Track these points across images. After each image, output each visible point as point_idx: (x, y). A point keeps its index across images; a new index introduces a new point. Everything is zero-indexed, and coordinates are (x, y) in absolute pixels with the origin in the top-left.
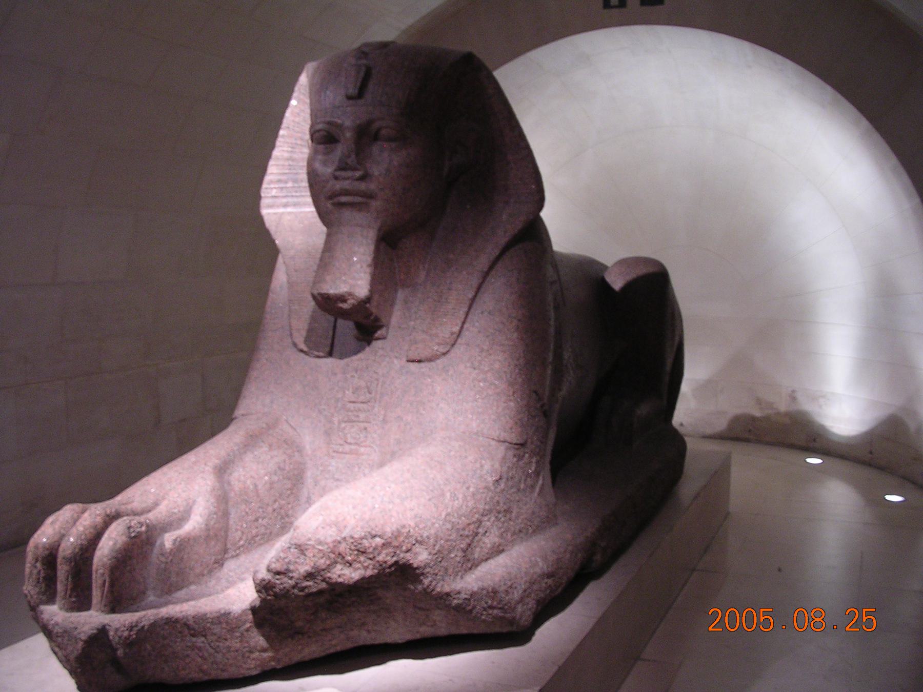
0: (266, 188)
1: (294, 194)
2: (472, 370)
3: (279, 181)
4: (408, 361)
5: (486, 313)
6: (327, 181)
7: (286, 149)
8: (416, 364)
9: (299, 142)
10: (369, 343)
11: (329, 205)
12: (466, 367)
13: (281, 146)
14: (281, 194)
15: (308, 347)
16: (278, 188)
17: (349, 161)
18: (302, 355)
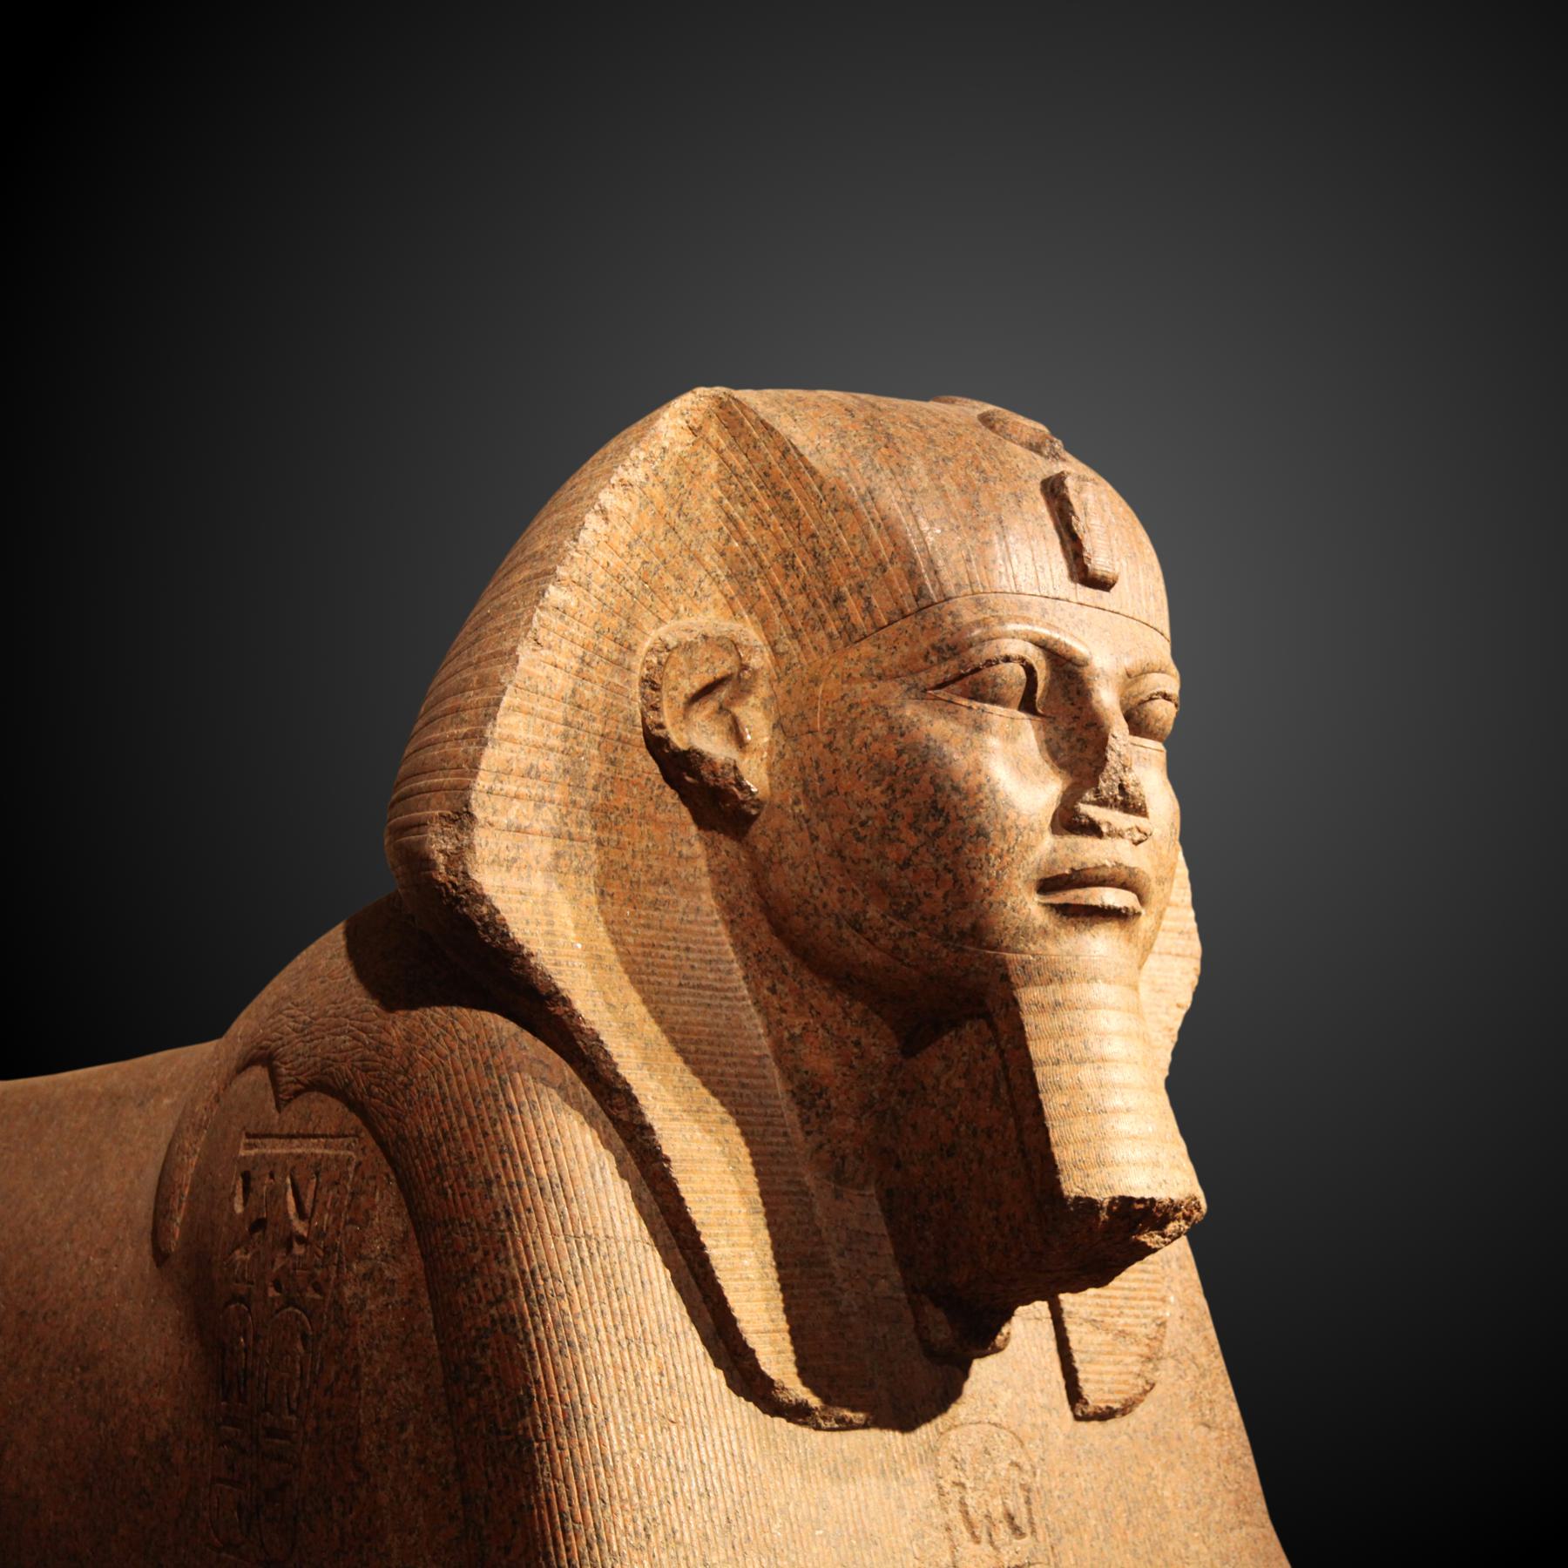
0: (490, 792)
1: (574, 830)
2: (1203, 1429)
3: (530, 773)
4: (1077, 1418)
5: (1174, 1265)
6: (1042, 832)
7: (561, 660)
8: (1095, 1423)
9: (607, 647)
10: (966, 1375)
11: (1032, 908)
12: (1196, 1425)
13: (550, 648)
14: (538, 826)
15: (816, 1392)
16: (530, 798)
17: (1129, 778)
18: (780, 1423)
